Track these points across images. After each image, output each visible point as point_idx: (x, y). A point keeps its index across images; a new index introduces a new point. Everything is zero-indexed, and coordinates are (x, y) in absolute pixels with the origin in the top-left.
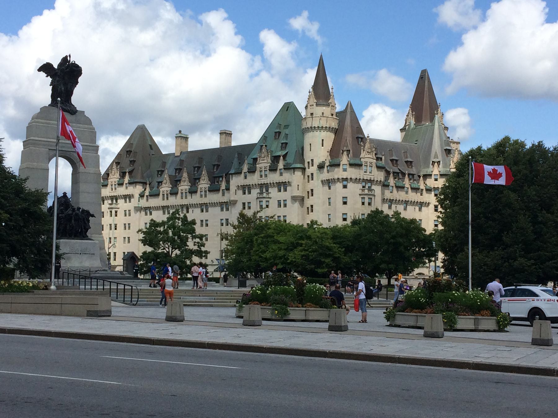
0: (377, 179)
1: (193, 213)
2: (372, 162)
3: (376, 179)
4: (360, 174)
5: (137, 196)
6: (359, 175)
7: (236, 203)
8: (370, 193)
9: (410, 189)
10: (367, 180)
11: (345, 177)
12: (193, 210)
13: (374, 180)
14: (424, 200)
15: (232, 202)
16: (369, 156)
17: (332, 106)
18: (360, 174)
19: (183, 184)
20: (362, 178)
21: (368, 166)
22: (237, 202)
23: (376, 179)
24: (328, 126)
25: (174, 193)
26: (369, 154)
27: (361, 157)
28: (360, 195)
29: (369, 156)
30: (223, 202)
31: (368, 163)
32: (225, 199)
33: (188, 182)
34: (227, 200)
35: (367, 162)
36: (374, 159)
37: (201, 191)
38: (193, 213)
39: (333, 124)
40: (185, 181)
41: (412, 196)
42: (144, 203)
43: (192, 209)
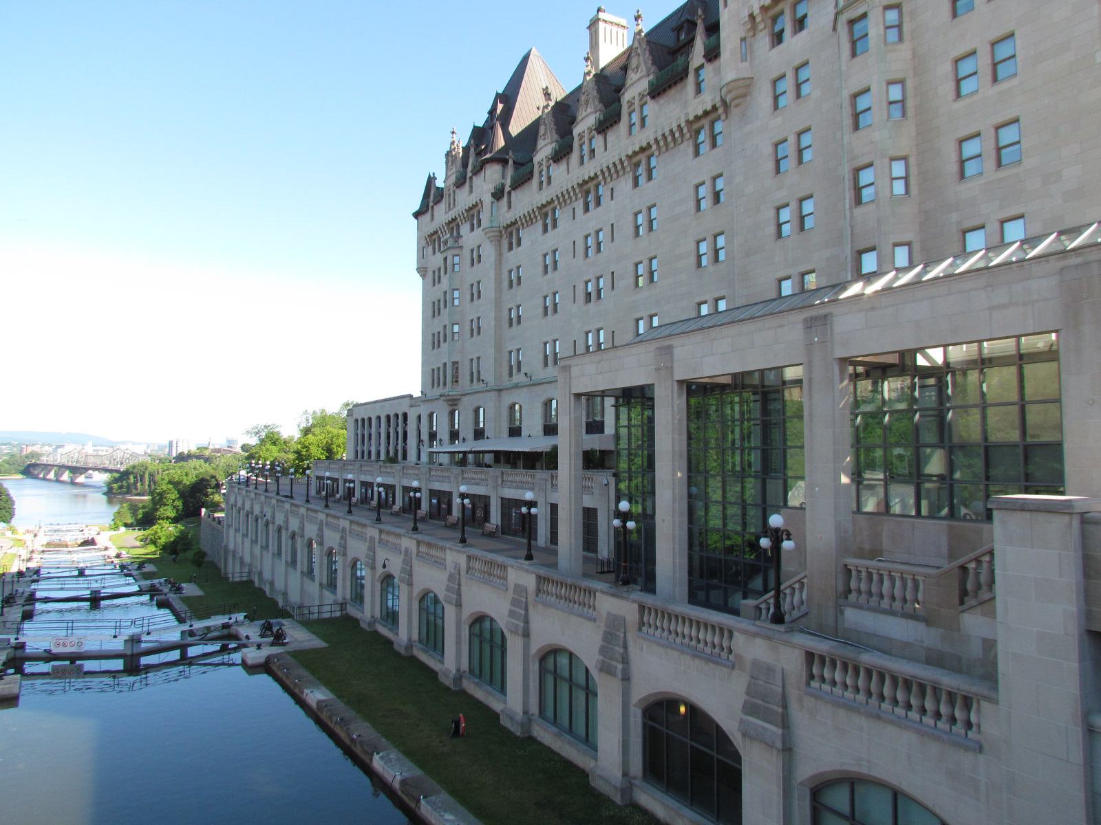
1: (612, 198)
5: (487, 199)
7: (744, 96)
12: (612, 189)
15: (729, 92)
19: (584, 114)
22: (749, 86)
25: (561, 154)
30: (700, 113)
32: (707, 100)
33: (597, 103)
34: (713, 100)
37: (630, 114)
38: (612, 198)
40: (587, 103)
42: (507, 217)
43: (611, 185)
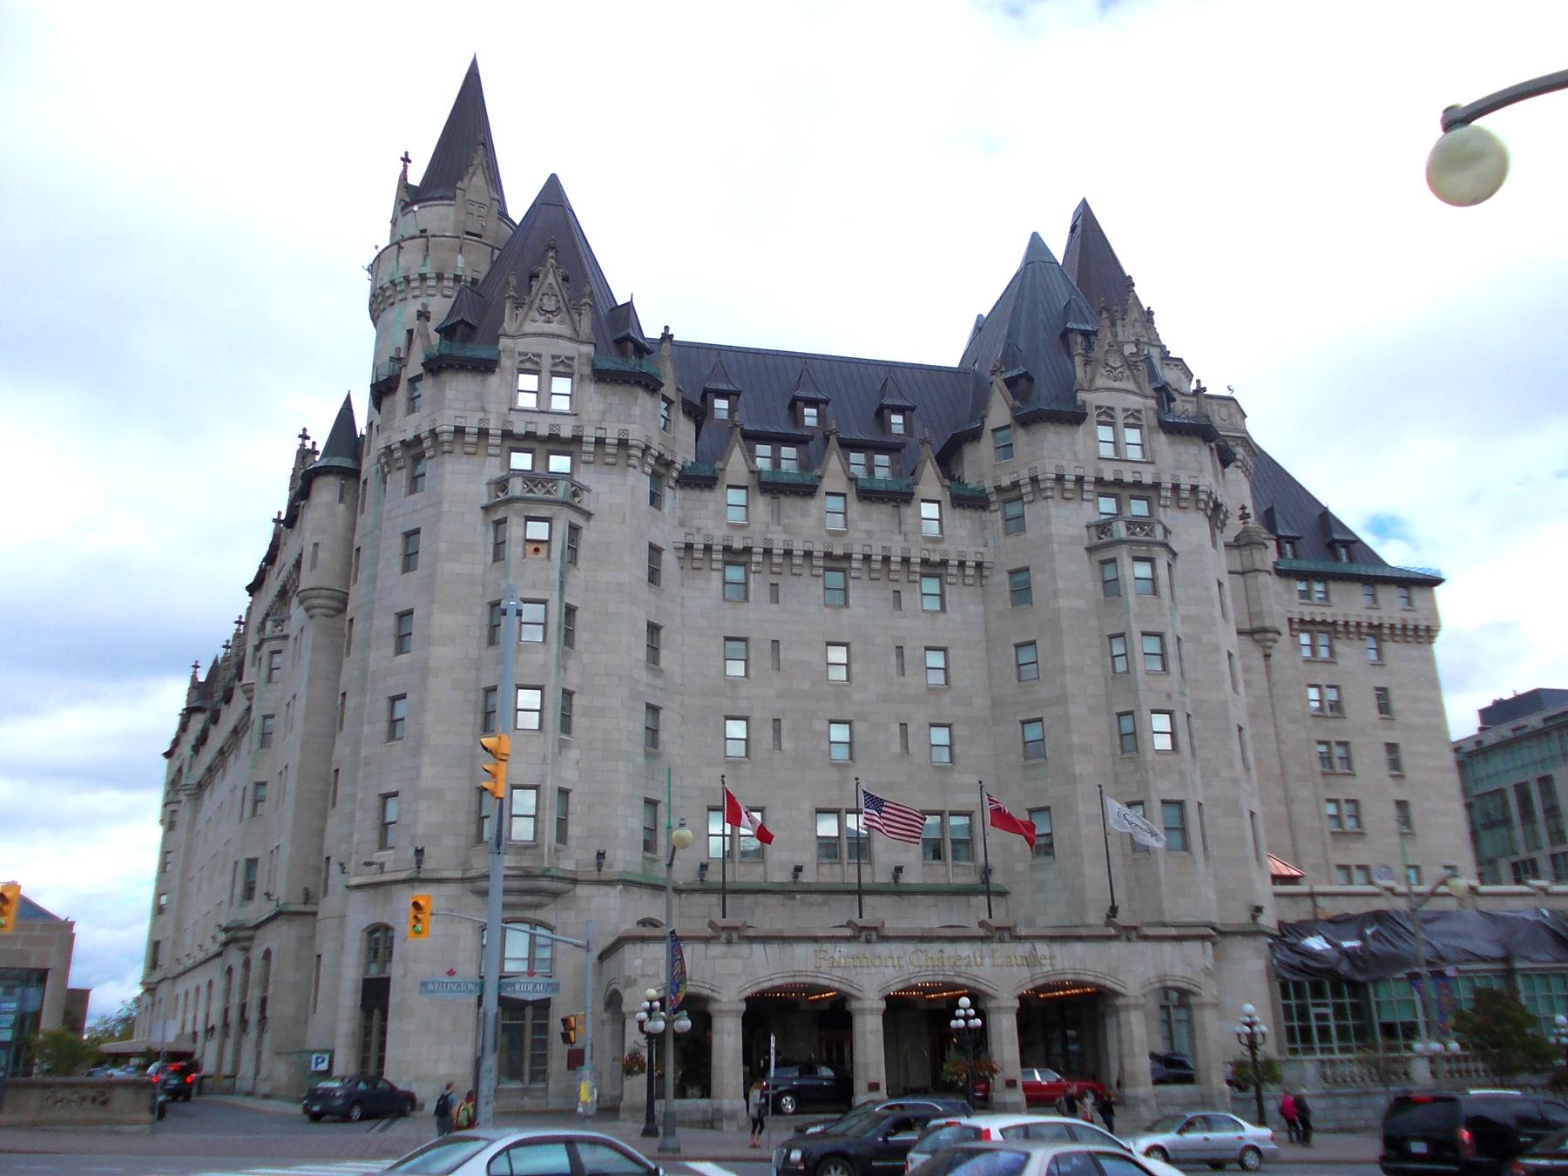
0: (600, 434)
2: (572, 359)
3: (590, 434)
4: (483, 410)
6: (481, 415)
8: (539, 494)
9: (852, 496)
10: (530, 436)
11: (409, 436)
13: (577, 440)
14: (945, 552)
16: (554, 327)
17: (472, 202)
18: (483, 410)
20: (494, 426)
21: (546, 374)
23: (590, 434)
24: (428, 270)
26: (549, 322)
27: (500, 332)
28: (486, 509)
29: (554, 327)
31: (546, 363)
35: (539, 356)
36: (582, 342)
39: (460, 261)
41: (869, 533)
